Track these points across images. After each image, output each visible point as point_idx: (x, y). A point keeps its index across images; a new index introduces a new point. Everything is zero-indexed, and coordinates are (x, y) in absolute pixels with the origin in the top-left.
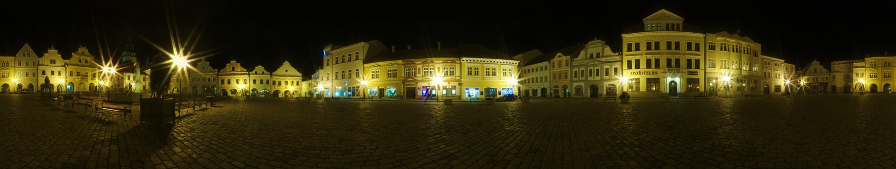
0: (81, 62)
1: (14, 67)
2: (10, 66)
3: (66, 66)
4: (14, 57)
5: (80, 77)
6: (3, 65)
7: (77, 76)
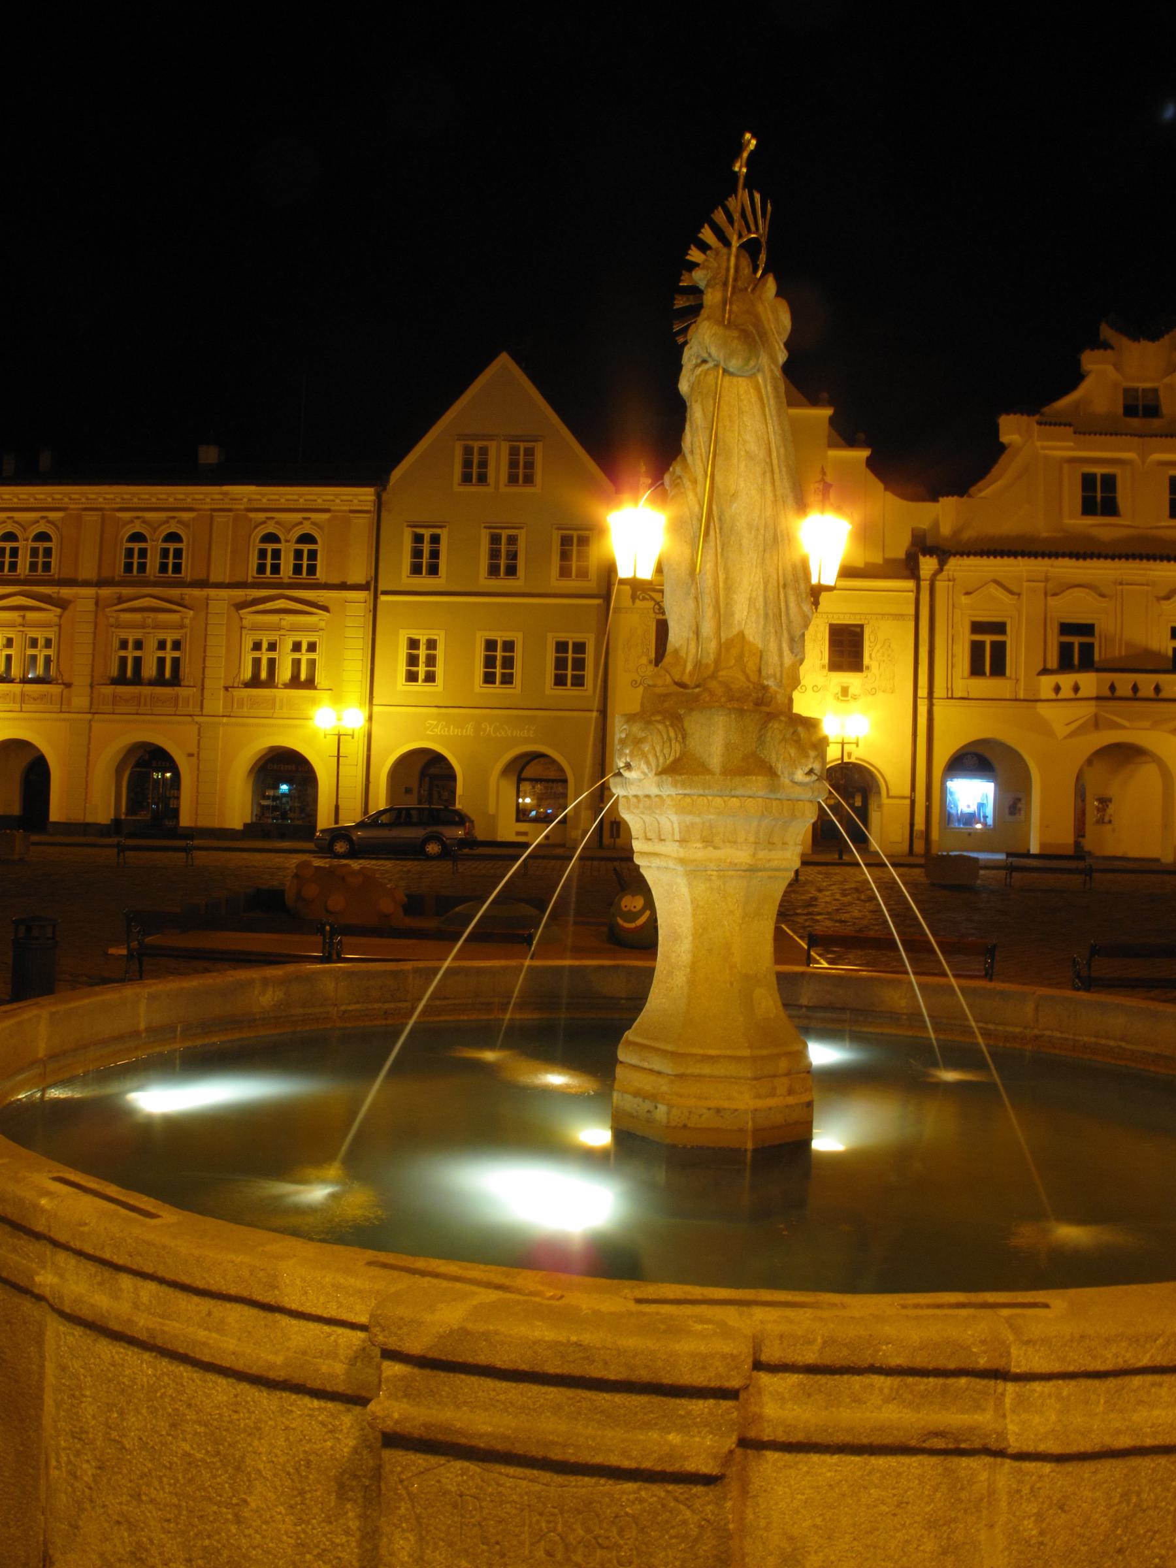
0: (1110, 508)
1: (371, 586)
2: (321, 575)
3: (928, 565)
4: (365, 495)
5: (1089, 682)
6: (268, 563)
7: (1066, 664)
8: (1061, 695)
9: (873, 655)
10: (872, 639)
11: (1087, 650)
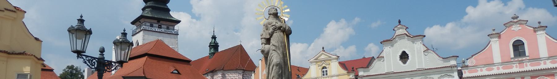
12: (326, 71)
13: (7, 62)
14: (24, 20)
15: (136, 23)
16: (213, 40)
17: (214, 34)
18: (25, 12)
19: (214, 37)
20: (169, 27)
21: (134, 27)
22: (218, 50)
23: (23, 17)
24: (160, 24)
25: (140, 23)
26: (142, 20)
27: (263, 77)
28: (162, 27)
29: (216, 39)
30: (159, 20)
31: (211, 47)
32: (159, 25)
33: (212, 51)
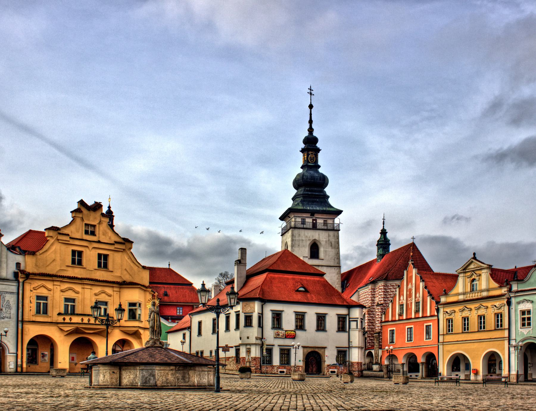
8: (66, 321)
9: (4, 306)
10: (3, 300)
11: (73, 307)
12: (476, 284)
13: (120, 292)
14: (132, 250)
15: (285, 219)
16: (382, 237)
17: (383, 227)
18: (133, 242)
19: (384, 232)
20: (326, 221)
21: (284, 224)
22: (388, 251)
23: (131, 248)
24: (314, 218)
25: (290, 219)
26: (292, 215)
27: (408, 293)
28: (318, 222)
29: (387, 234)
30: (312, 213)
31: (379, 246)
32: (313, 220)
33: (381, 252)
